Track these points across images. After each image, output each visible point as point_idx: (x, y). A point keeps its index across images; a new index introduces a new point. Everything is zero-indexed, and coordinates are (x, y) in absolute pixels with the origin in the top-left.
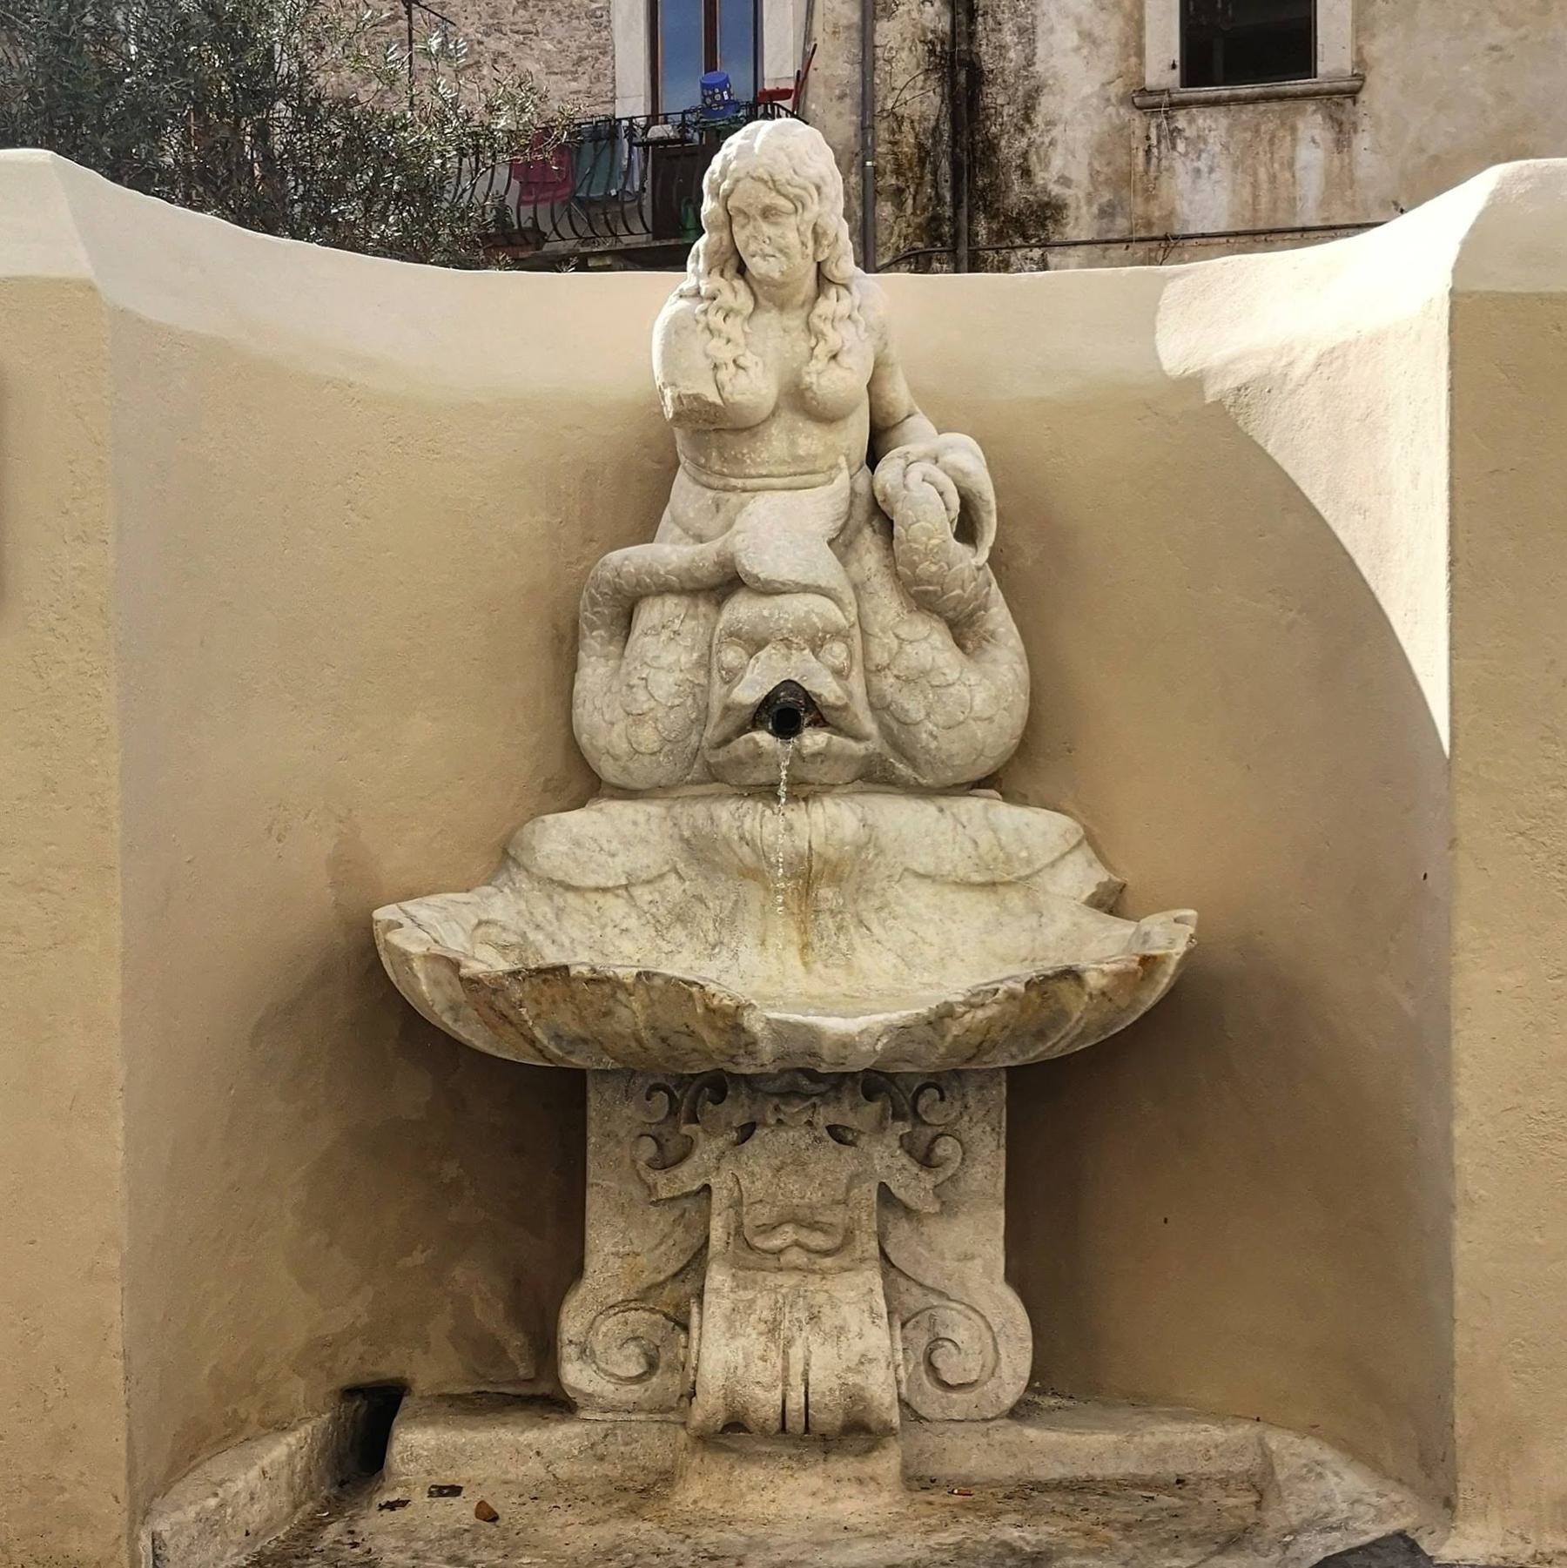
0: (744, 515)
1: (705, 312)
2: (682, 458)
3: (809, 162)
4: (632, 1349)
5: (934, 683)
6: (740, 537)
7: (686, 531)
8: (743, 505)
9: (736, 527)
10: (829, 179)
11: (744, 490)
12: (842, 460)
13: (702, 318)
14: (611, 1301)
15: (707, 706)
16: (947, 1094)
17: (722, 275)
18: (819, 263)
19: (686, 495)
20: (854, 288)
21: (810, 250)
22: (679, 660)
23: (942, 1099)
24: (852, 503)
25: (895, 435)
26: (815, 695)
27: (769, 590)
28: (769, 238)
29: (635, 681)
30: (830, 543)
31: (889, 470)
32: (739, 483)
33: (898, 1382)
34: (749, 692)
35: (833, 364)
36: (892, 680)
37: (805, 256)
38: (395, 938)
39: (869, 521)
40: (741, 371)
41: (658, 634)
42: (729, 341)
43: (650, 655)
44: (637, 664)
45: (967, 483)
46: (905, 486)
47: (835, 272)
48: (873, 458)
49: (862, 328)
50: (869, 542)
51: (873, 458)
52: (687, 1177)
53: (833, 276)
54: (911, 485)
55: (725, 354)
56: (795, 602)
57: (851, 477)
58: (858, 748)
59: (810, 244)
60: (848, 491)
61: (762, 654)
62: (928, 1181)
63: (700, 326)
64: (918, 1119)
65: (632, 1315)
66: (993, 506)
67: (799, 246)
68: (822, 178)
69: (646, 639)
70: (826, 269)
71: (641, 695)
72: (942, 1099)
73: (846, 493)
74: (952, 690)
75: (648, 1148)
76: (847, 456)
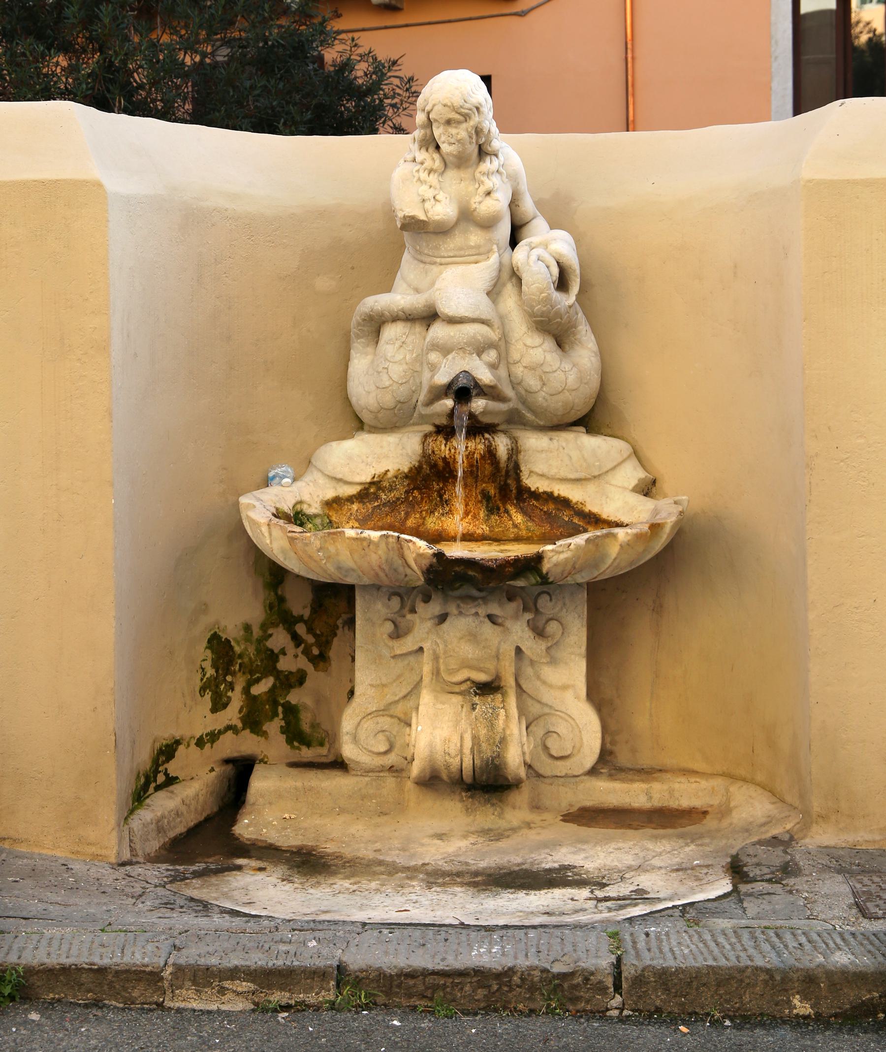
1: (418, 171)
2: (407, 245)
3: (473, 95)
4: (381, 737)
5: (545, 370)
6: (438, 292)
7: (409, 286)
8: (441, 273)
9: (436, 286)
11: (441, 264)
12: (495, 247)
13: (416, 174)
14: (369, 711)
15: (421, 383)
16: (553, 597)
17: (427, 150)
18: (480, 146)
19: (409, 267)
20: (500, 155)
22: (405, 358)
23: (551, 600)
24: (500, 271)
25: (525, 231)
26: (479, 379)
27: (453, 321)
29: (380, 369)
30: (488, 294)
31: (520, 253)
32: (438, 260)
33: (524, 753)
34: (443, 378)
35: (488, 198)
36: (521, 369)
37: (470, 143)
38: (252, 514)
40: (437, 203)
41: (394, 344)
42: (431, 187)
43: (389, 355)
44: (382, 360)
45: (562, 260)
46: (528, 263)
49: (504, 177)
50: (509, 289)
51: (514, 242)
52: (408, 644)
54: (531, 263)
55: (429, 194)
56: (468, 328)
57: (500, 256)
58: (503, 407)
59: (474, 137)
60: (498, 264)
61: (450, 357)
62: (542, 645)
63: (415, 179)
64: (537, 611)
65: (381, 720)
66: (578, 272)
68: (480, 104)
69: (387, 346)
70: (484, 148)
71: (385, 378)
72: (551, 600)
73: (496, 266)
74: (555, 374)
75: (389, 627)
76: (497, 245)
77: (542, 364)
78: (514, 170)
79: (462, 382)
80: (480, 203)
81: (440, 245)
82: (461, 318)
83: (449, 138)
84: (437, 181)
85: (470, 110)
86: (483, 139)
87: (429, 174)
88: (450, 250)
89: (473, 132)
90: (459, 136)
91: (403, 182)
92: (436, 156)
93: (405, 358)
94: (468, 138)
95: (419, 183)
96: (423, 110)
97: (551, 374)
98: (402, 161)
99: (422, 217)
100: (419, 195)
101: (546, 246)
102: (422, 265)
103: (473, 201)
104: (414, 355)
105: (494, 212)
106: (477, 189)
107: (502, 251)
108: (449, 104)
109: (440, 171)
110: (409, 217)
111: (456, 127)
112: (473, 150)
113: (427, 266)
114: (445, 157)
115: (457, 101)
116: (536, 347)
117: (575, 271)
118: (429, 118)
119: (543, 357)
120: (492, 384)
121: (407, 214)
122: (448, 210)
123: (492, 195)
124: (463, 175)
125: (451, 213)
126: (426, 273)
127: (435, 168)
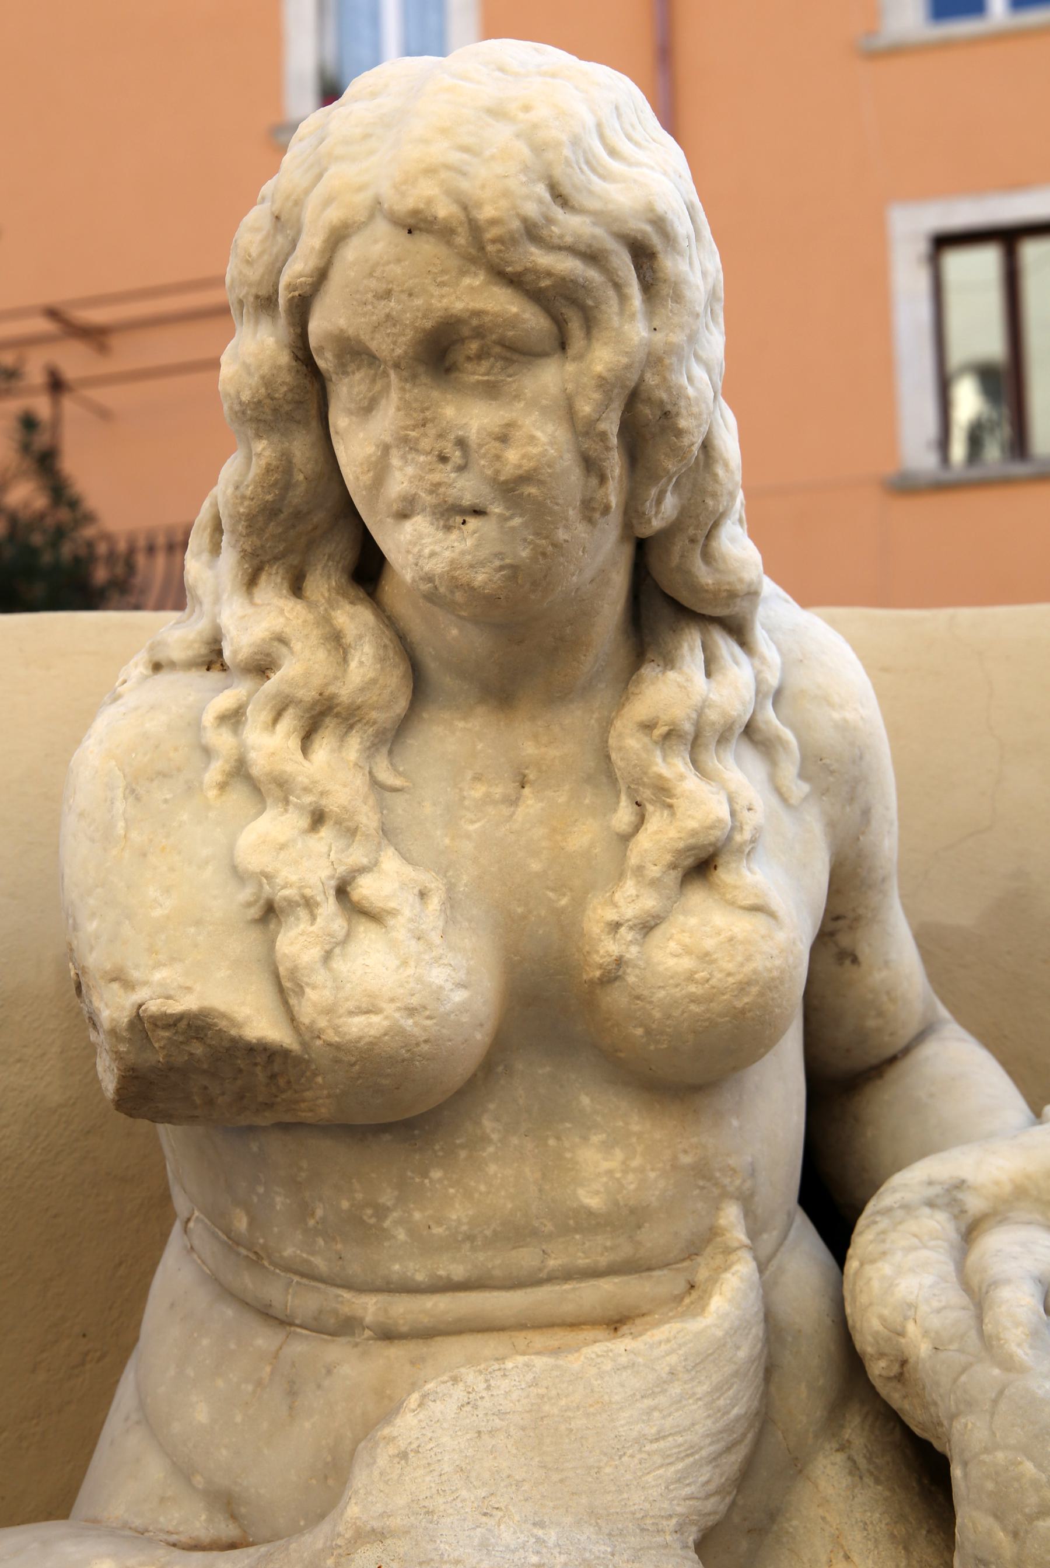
0: (383, 1458)
1: (234, 718)
2: (181, 1203)
10: (683, 227)
11: (388, 1335)
12: (731, 1215)
13: (223, 740)
17: (297, 588)
20: (760, 635)
21: (613, 495)
28: (461, 443)
35: (697, 897)
42: (318, 818)
47: (705, 576)
49: (789, 769)
53: (696, 588)
57: (761, 1268)
59: (615, 464)
60: (757, 1330)
63: (215, 772)
67: (575, 475)
68: (660, 223)
73: (746, 1349)
76: (746, 1201)
78: (843, 727)
80: (647, 926)
81: (382, 1212)
83: (445, 474)
84: (360, 781)
85: (593, 256)
86: (670, 505)
87: (307, 739)
88: (455, 1241)
89: (611, 426)
90: (512, 456)
91: (131, 791)
94: (568, 462)
95: (238, 796)
96: (266, 303)
98: (137, 668)
100: (239, 875)
102: (264, 1339)
105: (743, 987)
106: (626, 838)
107: (769, 1239)
108: (444, 209)
109: (386, 717)
110: (172, 1022)
111: (491, 391)
112: (601, 578)
113: (300, 1347)
114: (417, 628)
121: (154, 1007)
122: (438, 976)
123: (724, 875)
124: (530, 749)
125: (459, 996)
126: (292, 1393)
127: (346, 691)
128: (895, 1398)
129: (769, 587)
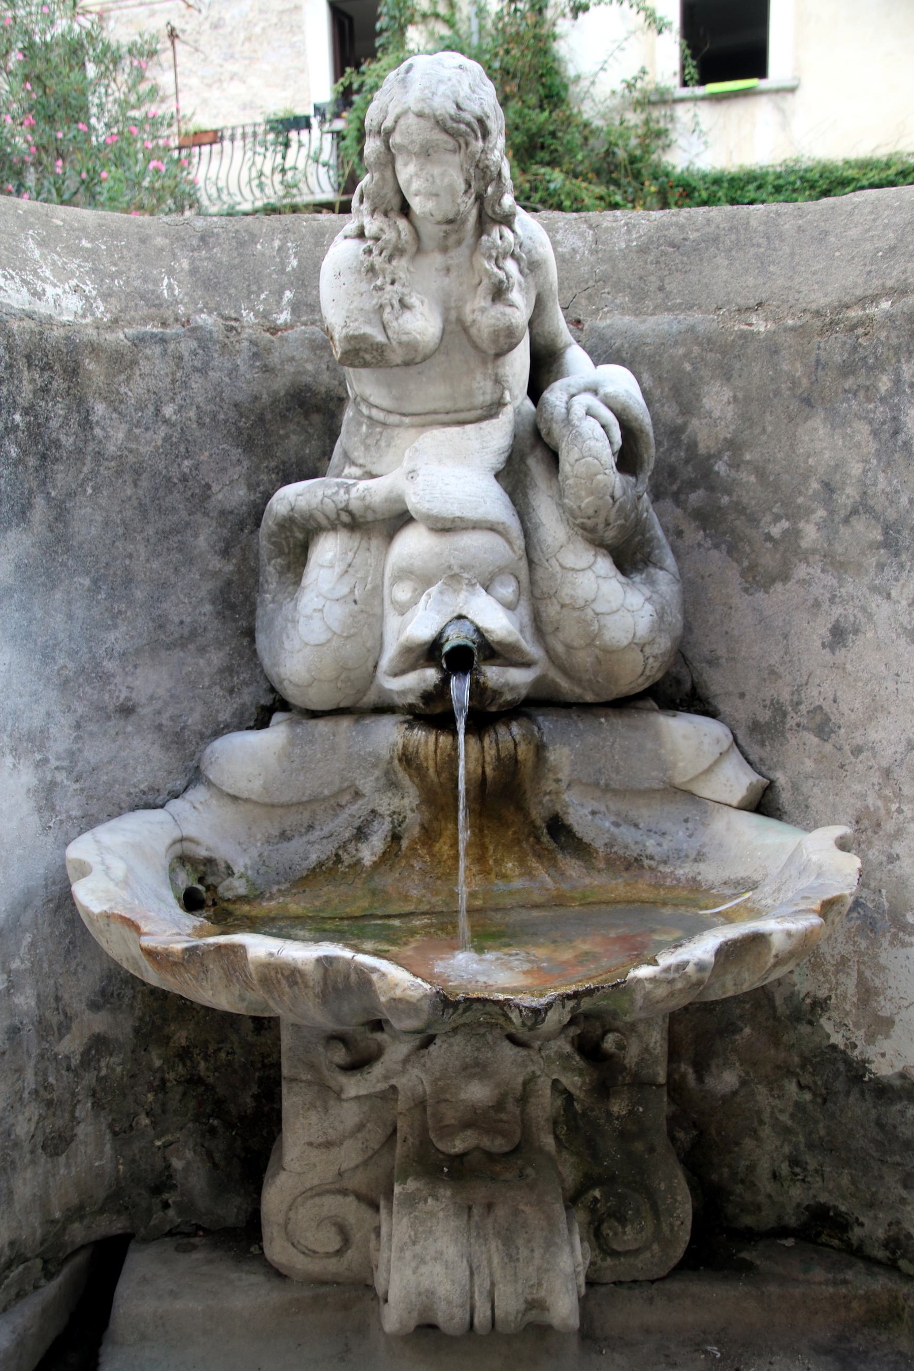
26: (487, 631)
39: (533, 447)
48: (535, 391)
66: (651, 434)
74: (616, 617)
77: (594, 600)
79: (455, 637)
80: (483, 310)
82: (453, 520)
92: (402, 223)
93: (352, 591)
97: (607, 617)
99: (380, 338)
101: (595, 392)
103: (468, 308)
104: (369, 587)
115: (444, 106)
116: (583, 570)
117: (647, 435)
118: (388, 148)
119: (594, 586)
120: (510, 639)
128: (547, 440)
129: (519, 209)
